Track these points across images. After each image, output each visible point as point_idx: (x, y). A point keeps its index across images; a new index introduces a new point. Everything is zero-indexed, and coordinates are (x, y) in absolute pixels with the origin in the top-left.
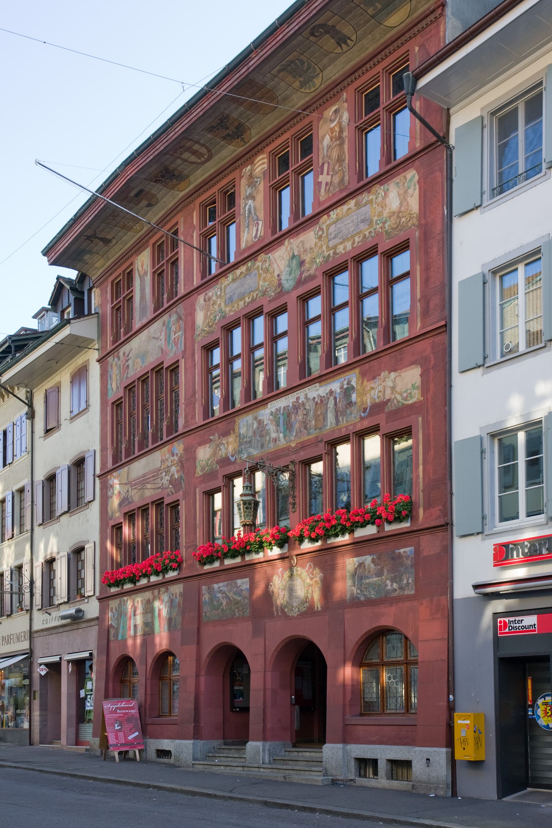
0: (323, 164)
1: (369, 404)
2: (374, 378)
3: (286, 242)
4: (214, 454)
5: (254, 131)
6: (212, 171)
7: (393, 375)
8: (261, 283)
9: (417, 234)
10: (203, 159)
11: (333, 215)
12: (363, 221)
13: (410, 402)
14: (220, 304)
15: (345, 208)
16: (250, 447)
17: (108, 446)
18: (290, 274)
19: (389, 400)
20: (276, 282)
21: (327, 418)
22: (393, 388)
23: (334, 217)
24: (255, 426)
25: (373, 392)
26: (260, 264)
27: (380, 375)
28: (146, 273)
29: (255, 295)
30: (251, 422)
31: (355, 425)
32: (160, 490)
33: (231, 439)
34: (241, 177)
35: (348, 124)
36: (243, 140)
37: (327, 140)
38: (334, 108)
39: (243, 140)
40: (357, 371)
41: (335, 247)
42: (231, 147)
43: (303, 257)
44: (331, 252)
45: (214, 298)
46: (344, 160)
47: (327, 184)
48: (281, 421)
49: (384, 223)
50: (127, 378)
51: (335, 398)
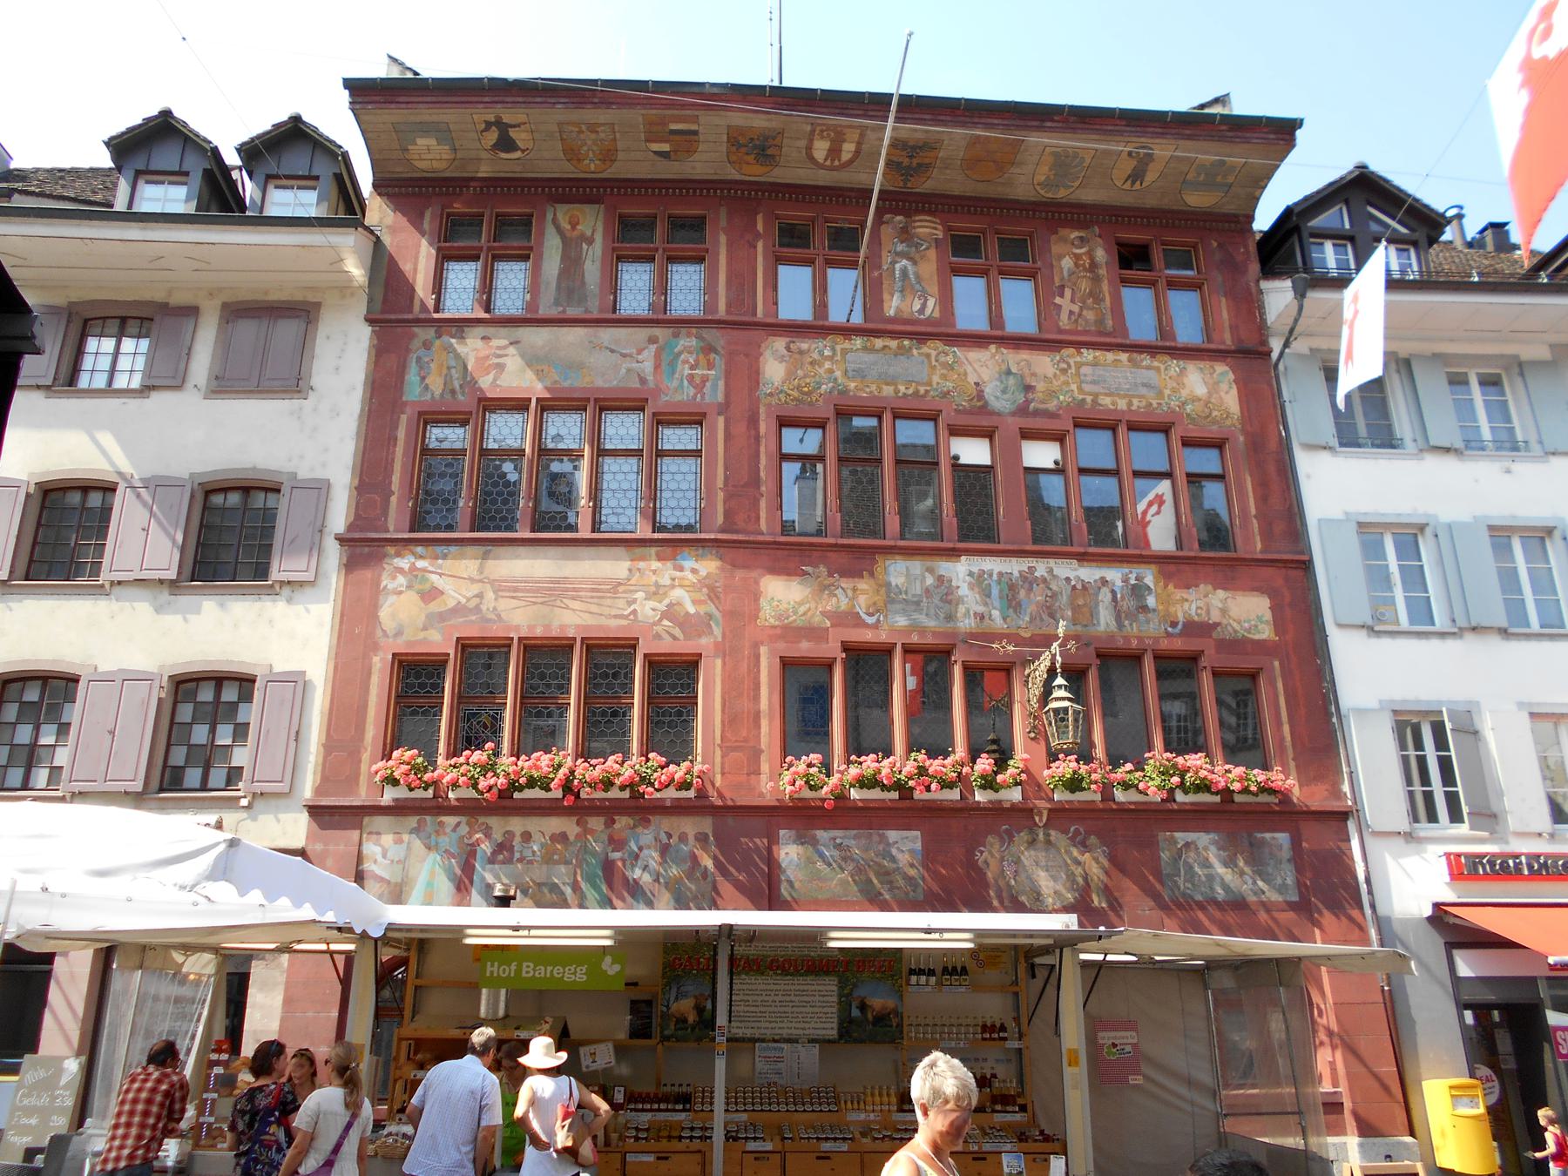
1: (1181, 619)
2: (1188, 587)
3: (993, 348)
7: (1221, 594)
8: (936, 379)
11: (1089, 355)
12: (1144, 385)
15: (1110, 356)
16: (919, 611)
18: (1004, 392)
19: (1217, 625)
20: (973, 391)
23: (1090, 357)
24: (930, 581)
25: (1186, 605)
29: (922, 390)
30: (918, 572)
31: (1156, 639)
33: (863, 585)
37: (1067, 263)
41: (1096, 395)
44: (1089, 399)
46: (1103, 300)
48: (995, 592)
51: (1113, 593)
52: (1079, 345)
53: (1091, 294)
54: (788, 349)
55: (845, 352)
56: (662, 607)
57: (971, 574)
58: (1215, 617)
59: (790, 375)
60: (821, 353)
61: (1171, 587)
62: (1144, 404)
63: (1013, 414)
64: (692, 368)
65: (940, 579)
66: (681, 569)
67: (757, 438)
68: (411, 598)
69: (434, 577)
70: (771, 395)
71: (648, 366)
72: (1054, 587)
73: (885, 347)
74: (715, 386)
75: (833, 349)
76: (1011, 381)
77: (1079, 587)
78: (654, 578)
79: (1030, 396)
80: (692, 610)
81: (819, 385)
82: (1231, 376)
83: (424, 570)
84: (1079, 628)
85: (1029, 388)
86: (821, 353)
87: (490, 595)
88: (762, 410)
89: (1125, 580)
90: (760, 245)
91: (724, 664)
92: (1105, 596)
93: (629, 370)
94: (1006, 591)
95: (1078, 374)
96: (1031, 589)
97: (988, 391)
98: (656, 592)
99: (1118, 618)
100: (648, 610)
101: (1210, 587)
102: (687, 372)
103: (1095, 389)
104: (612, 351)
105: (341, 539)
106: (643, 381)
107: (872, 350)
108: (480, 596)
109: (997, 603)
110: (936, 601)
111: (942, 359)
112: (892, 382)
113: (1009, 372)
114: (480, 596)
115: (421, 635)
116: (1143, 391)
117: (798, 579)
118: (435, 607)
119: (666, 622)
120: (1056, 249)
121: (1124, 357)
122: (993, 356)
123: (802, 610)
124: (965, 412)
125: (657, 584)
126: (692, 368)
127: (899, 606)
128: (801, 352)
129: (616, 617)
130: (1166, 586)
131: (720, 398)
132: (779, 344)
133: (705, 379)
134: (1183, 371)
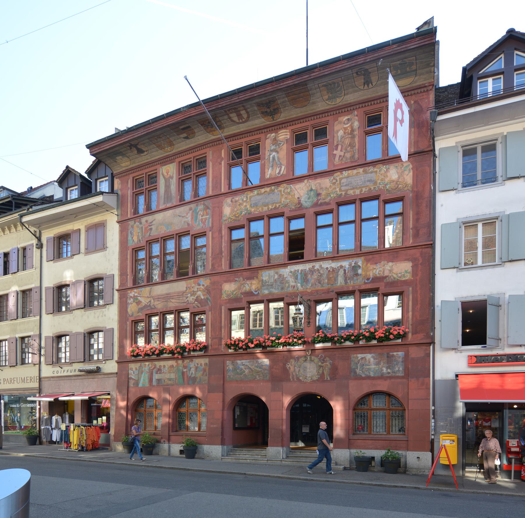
0: (338, 145)
1: (371, 276)
2: (376, 263)
3: (306, 181)
4: (239, 288)
5: (282, 115)
6: (242, 130)
7: (390, 264)
8: (283, 200)
9: (411, 195)
10: (241, 121)
11: (345, 173)
12: (369, 181)
13: (404, 279)
14: (246, 206)
15: (355, 171)
16: (273, 288)
17: (128, 273)
18: (309, 199)
19: (387, 277)
20: (296, 201)
21: (338, 279)
22: (390, 271)
23: (346, 174)
24: (276, 277)
25: (375, 271)
26: (283, 189)
27: (380, 262)
28: (172, 177)
29: (277, 205)
30: (272, 274)
31: (360, 286)
32: (185, 304)
33: (254, 282)
34: (266, 139)
35: (358, 128)
36: (273, 118)
37: (341, 133)
38: (346, 118)
39: (273, 118)
40: (363, 258)
41: (347, 191)
42: (263, 120)
43: (320, 191)
44: (343, 193)
45: (241, 201)
46: (355, 146)
47: (340, 156)
48: (299, 277)
49: (386, 185)
50: (150, 236)
51: (345, 270)
52: (341, 170)
53: (350, 145)
54: (232, 201)
55: (251, 197)
56: (195, 298)
57: (291, 272)
58: (386, 273)
59: (232, 211)
60: (243, 200)
61: (369, 265)
62: (368, 189)
63: (312, 207)
64: (202, 216)
65: (280, 276)
66: (199, 285)
67: (222, 237)
68: (134, 304)
69: (139, 298)
70: (226, 220)
71: (190, 218)
72: (321, 272)
73: (265, 191)
74: (209, 222)
75: (247, 197)
76: (312, 193)
77: (331, 270)
78: (193, 289)
79: (319, 198)
80: (203, 297)
81: (242, 212)
82: (411, 166)
83: (137, 296)
84: (330, 286)
85: (319, 195)
86: (243, 200)
87: (152, 301)
88: (223, 226)
89: (350, 265)
90: (223, 163)
91: (212, 313)
92: (341, 272)
93: (184, 222)
94: (303, 276)
95: (340, 183)
96: (313, 274)
97: (302, 200)
98: (193, 293)
99: (346, 280)
100: (191, 299)
101: (386, 262)
102: (201, 218)
103: (347, 188)
104: (180, 216)
105: (117, 290)
106: (188, 224)
107: (261, 194)
108: (150, 302)
109: (300, 281)
110: (278, 284)
111: (286, 191)
112: (267, 205)
113: (311, 190)
114: (150, 302)
115: (138, 315)
116: (368, 184)
117: (233, 283)
118: (140, 306)
119: (196, 302)
120: (336, 128)
121: (361, 170)
122: (306, 184)
123: (235, 293)
124: (293, 210)
125: (193, 291)
126: (202, 216)
127: (266, 287)
128: (236, 201)
129: (183, 303)
130: (367, 264)
131: (210, 224)
132: (229, 200)
133: (206, 219)
134: (388, 170)
